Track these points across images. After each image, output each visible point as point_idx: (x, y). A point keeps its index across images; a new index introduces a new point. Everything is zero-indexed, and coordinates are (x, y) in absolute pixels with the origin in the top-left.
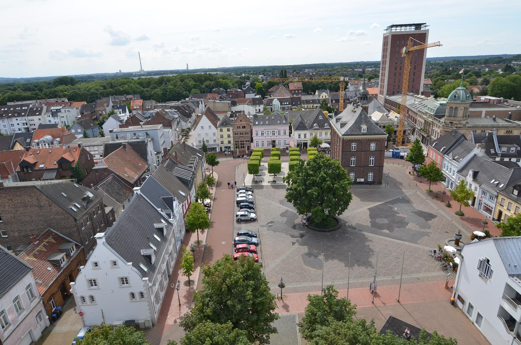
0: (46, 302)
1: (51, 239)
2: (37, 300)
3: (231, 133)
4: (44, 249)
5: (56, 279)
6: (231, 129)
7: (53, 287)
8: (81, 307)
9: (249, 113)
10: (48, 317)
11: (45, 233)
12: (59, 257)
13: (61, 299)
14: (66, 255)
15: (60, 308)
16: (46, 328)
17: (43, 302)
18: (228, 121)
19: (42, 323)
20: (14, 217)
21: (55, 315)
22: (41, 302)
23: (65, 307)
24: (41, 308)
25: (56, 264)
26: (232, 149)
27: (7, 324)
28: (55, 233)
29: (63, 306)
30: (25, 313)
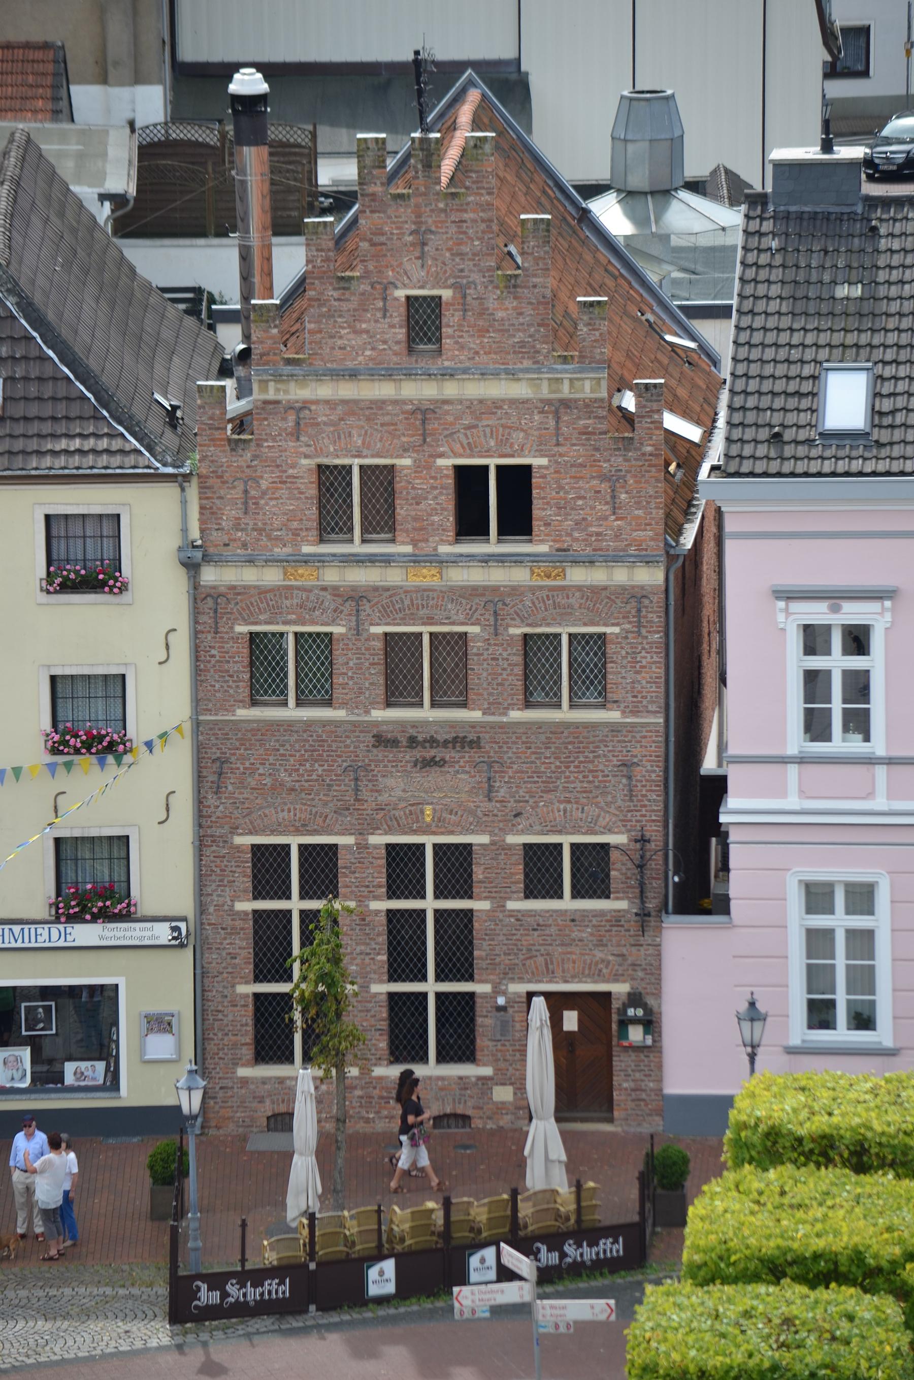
3: (143, 639)
6: (151, 524)
9: (649, 114)
18: (86, 320)
26: (153, 1070)
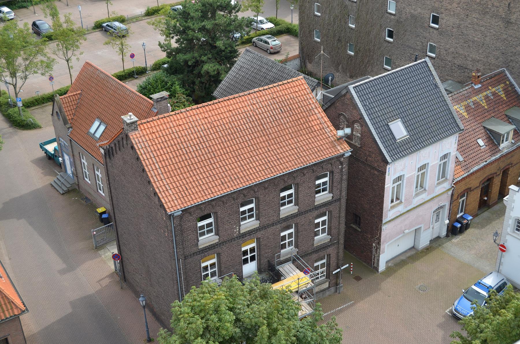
0: (455, 197)
1: (499, 90)
2: (446, 185)
4: (484, 104)
5: (485, 166)
7: (473, 177)
8: (508, 238)
10: (447, 222)
11: (495, 75)
12: (504, 129)
13: (476, 204)
14: (515, 130)
15: (470, 218)
16: (438, 238)
17: (452, 195)
19: (437, 225)
20: (459, 27)
21: (459, 225)
22: (450, 193)
23: (477, 220)
24: (446, 201)
25: (493, 139)
27: (397, 199)
28: (510, 83)
29: (475, 216)
30: (424, 197)
